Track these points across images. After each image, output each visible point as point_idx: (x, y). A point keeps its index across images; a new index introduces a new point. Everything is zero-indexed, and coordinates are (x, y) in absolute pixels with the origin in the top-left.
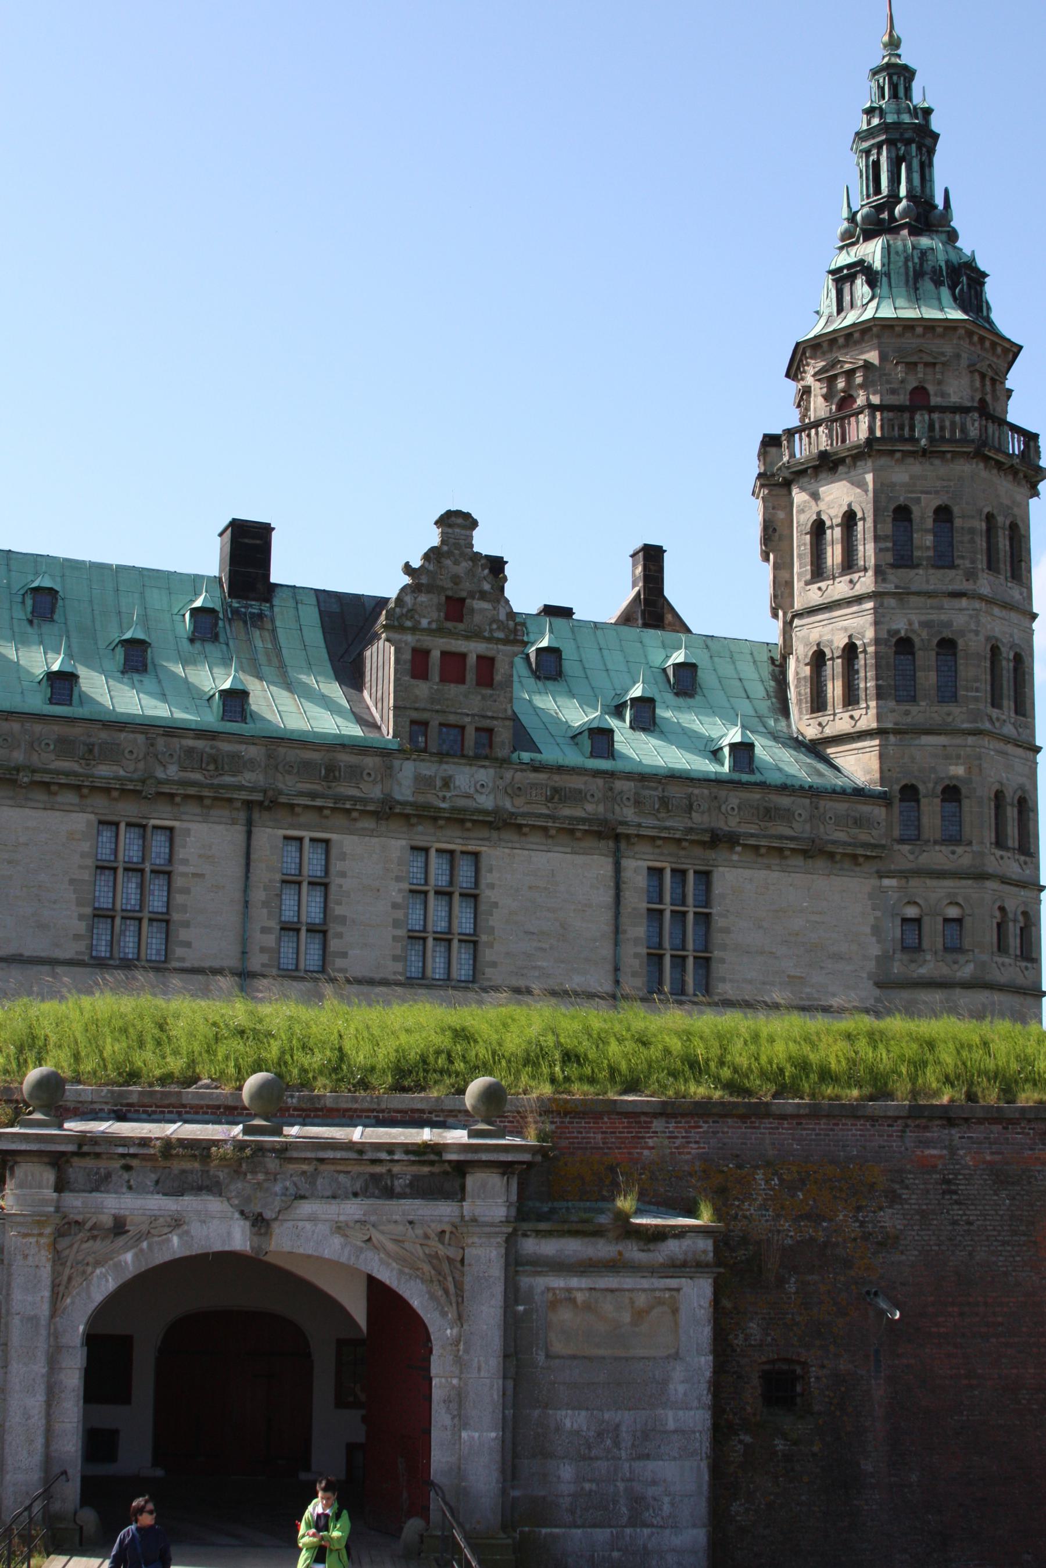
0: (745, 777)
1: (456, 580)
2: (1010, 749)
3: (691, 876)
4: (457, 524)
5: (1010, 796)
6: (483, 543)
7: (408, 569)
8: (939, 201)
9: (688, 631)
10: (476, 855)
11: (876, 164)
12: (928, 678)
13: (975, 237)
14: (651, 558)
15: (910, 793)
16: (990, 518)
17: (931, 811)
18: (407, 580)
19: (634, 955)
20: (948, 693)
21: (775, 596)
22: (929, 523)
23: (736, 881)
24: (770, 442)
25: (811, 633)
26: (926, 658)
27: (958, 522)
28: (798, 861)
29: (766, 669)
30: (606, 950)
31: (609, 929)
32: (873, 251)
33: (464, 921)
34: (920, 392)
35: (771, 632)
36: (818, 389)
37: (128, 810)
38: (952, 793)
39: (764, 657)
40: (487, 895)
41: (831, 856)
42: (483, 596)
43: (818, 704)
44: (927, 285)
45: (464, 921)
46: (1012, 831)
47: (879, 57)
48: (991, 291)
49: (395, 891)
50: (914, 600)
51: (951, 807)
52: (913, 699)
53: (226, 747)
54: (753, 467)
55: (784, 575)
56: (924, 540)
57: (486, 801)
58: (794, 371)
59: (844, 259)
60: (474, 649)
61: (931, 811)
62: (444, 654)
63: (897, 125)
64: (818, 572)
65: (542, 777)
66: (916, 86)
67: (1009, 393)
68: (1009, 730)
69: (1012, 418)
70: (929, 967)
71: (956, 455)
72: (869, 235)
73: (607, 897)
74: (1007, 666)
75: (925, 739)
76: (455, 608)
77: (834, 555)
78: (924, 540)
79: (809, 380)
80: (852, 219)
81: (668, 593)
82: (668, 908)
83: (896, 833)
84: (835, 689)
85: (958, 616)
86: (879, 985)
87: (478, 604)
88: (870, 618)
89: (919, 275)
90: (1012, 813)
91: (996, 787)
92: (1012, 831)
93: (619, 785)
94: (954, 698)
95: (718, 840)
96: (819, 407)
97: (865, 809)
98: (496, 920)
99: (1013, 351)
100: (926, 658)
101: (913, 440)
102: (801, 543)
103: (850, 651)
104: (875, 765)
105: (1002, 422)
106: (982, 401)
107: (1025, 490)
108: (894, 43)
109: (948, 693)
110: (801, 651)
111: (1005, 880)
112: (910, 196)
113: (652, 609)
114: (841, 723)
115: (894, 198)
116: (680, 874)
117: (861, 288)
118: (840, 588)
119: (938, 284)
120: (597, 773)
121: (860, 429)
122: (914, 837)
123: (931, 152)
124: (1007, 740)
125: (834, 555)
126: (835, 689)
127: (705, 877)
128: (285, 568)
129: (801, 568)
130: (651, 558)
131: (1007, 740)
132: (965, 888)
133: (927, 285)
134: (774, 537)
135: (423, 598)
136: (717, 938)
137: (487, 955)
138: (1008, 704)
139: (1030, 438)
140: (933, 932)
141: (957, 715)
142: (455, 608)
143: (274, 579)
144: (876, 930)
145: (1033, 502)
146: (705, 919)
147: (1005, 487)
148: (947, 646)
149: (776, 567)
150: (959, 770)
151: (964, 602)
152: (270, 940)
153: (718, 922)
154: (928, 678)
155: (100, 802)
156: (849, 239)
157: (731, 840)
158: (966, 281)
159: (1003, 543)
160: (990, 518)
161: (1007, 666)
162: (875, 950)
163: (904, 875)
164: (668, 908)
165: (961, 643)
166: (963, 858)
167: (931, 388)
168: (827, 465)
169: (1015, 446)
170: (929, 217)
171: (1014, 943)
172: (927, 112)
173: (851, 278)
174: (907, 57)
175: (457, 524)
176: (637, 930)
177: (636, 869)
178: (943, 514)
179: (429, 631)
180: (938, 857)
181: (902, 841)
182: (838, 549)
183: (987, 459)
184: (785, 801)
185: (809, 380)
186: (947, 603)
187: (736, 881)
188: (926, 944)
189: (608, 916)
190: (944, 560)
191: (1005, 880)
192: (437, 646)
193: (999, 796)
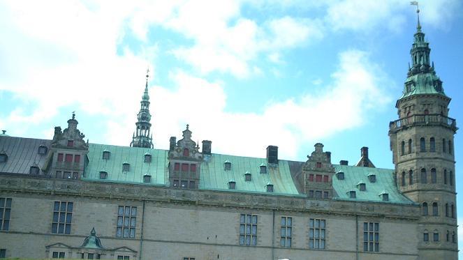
0: (386, 202)
1: (320, 159)
2: (450, 194)
3: (374, 224)
4: (319, 146)
5: (450, 205)
6: (325, 150)
7: (308, 156)
8: (431, 65)
9: (374, 167)
11: (416, 57)
12: (429, 178)
13: (440, 74)
14: (365, 150)
15: (425, 204)
16: (444, 140)
17: (430, 209)
18: (308, 159)
19: (361, 243)
20: (434, 181)
21: (393, 159)
22: (429, 141)
23: (385, 226)
24: (392, 123)
25: (402, 167)
26: (429, 173)
27: (436, 141)
28: (399, 220)
29: (392, 176)
30: (355, 241)
31: (355, 237)
32: (416, 78)
33: (322, 236)
34: (426, 110)
35: (393, 167)
36: (403, 110)
37: (247, 212)
38: (435, 204)
39: (391, 173)
40: (327, 229)
41: (406, 219)
42: (325, 162)
43: (403, 184)
44: (428, 85)
45: (322, 236)
46: (450, 213)
47: (416, 31)
48: (444, 86)
49: (307, 229)
50: (425, 160)
51: (435, 208)
52: (426, 183)
53: (268, 197)
54: (388, 129)
55: (395, 154)
56: (428, 145)
57: (327, 209)
58: (397, 106)
59: (408, 80)
60: (323, 174)
61: (430, 209)
62: (317, 175)
63: (421, 48)
64: (403, 154)
65: (339, 203)
66: (425, 37)
67: (448, 110)
68: (450, 190)
69: (449, 116)
70: (431, 245)
71: (435, 125)
72: (414, 74)
73: (355, 229)
74: (448, 174)
75: (429, 192)
76: (319, 164)
77: (407, 149)
78: (428, 145)
79: (401, 108)
80: (410, 70)
81: (369, 158)
82: (369, 231)
83: (422, 214)
84: (407, 181)
85: (437, 164)
86: (419, 249)
87: (324, 164)
88: (415, 164)
89: (426, 83)
90: (450, 209)
91: (446, 202)
92: (450, 213)
93: (357, 204)
94: (435, 182)
96: (403, 115)
97: (414, 208)
98: (329, 235)
99: (449, 100)
100: (429, 173)
101: (425, 122)
102: (399, 146)
103: (411, 171)
104: (417, 198)
105: (446, 117)
106: (442, 112)
107: (452, 132)
109: (434, 181)
110: (400, 172)
111: (448, 225)
112: (424, 64)
113: (366, 162)
114: (409, 188)
115: (420, 65)
116: (371, 224)
117: (412, 87)
118: (408, 157)
119: (430, 85)
120: (352, 202)
121: (413, 120)
122: (426, 215)
123: (429, 53)
124: (448, 192)
125: (407, 149)
126: (407, 181)
127: (377, 224)
128: (281, 156)
129: (399, 152)
130: (365, 150)
131: (448, 192)
132: (439, 227)
133: (428, 85)
134: (392, 145)
135: (312, 163)
136: (380, 238)
137: (327, 243)
138: (449, 184)
139: (454, 120)
140: (431, 237)
141: (437, 186)
142: (319, 164)
143: (279, 158)
144: (418, 236)
145: (455, 135)
146: (377, 234)
147: (448, 133)
148: (434, 170)
149: (393, 152)
150: (437, 199)
151: (438, 160)
152: (279, 240)
153: (380, 235)
154: (429, 178)
155: (241, 210)
156: (409, 75)
157: (383, 216)
158: (438, 84)
159: (447, 145)
160: (444, 140)
161: (448, 174)
162: (418, 241)
163: (425, 223)
164: (369, 231)
165: (437, 169)
166: (438, 219)
167: (429, 110)
168: (405, 128)
169: (450, 123)
170: (428, 69)
171: (451, 239)
172: (428, 44)
173: (410, 84)
174: (423, 31)
175: (319, 146)
176: (362, 237)
177: (361, 223)
178: (432, 139)
179: (315, 171)
180: (432, 219)
181: (424, 215)
182: (408, 148)
183: (443, 126)
184: (396, 207)
185: (401, 108)
186: (433, 160)
187: (385, 226)
188: (430, 239)
189: (355, 233)
190: (433, 150)
191: (448, 225)
192: (315, 174)
193: (447, 204)
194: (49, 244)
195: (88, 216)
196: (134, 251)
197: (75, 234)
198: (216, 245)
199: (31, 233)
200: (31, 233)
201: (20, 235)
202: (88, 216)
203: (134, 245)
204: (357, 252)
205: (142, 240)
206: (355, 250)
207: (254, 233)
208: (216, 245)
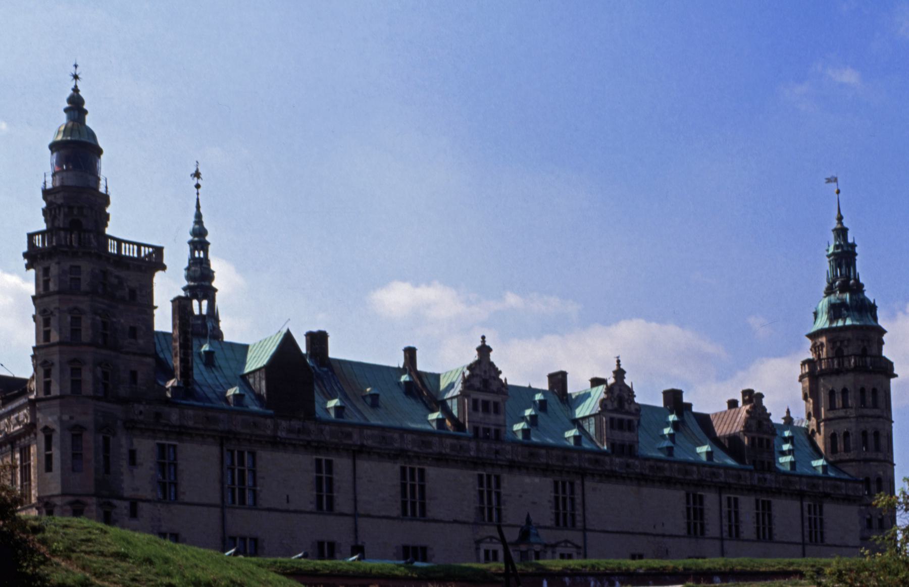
10: (174, 446)
23: (829, 508)
95: (827, 495)
108: (840, 219)
187: (829, 508)
194: (478, 537)
195: (520, 496)
196: (577, 547)
197: (509, 522)
198: (664, 536)
199: (455, 522)
200: (455, 522)
201: (442, 525)
202: (520, 496)
203: (575, 537)
204: (804, 544)
205: (585, 530)
206: (801, 541)
207: (172, 478)
208: (664, 536)
